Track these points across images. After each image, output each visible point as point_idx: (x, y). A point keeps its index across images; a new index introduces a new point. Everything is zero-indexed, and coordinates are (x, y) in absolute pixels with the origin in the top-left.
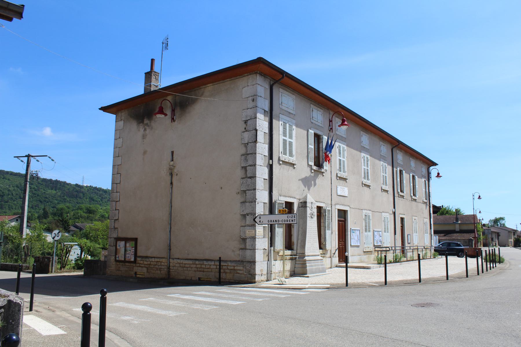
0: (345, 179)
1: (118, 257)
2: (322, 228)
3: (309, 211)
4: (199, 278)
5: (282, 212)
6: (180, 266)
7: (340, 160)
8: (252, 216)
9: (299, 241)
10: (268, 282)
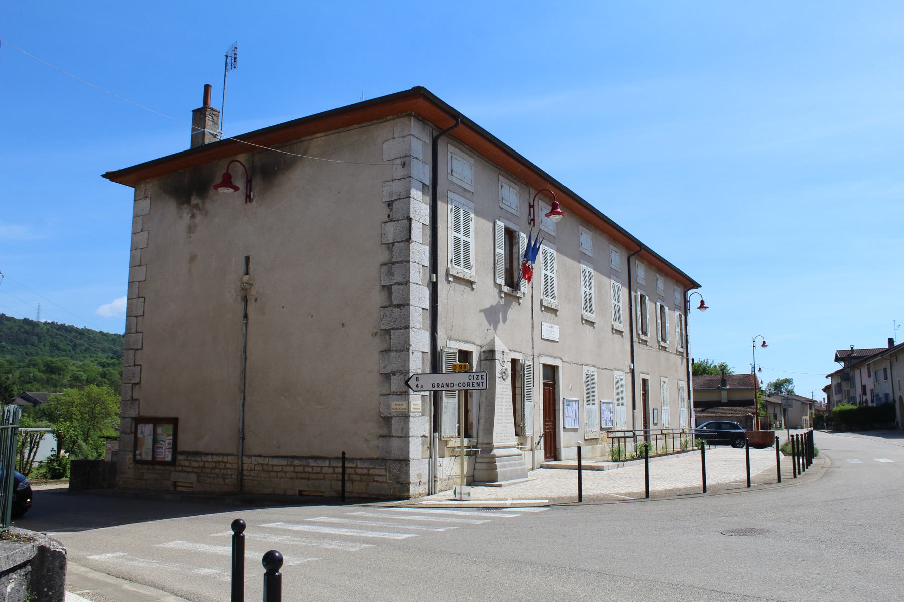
1: (140, 454)
2: (518, 398)
3: (498, 368)
4: (300, 491)
5: (458, 368)
6: (263, 470)
7: (546, 276)
8: (402, 376)
9: (482, 422)
10: (431, 497)
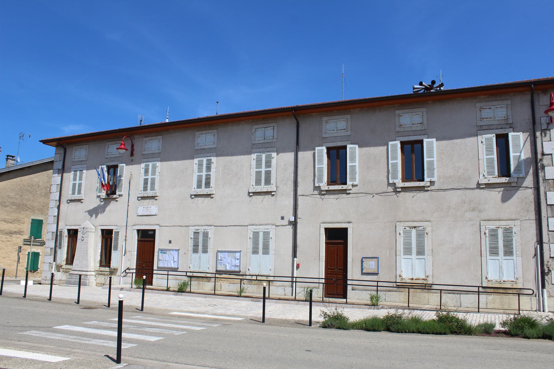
0: (153, 197)
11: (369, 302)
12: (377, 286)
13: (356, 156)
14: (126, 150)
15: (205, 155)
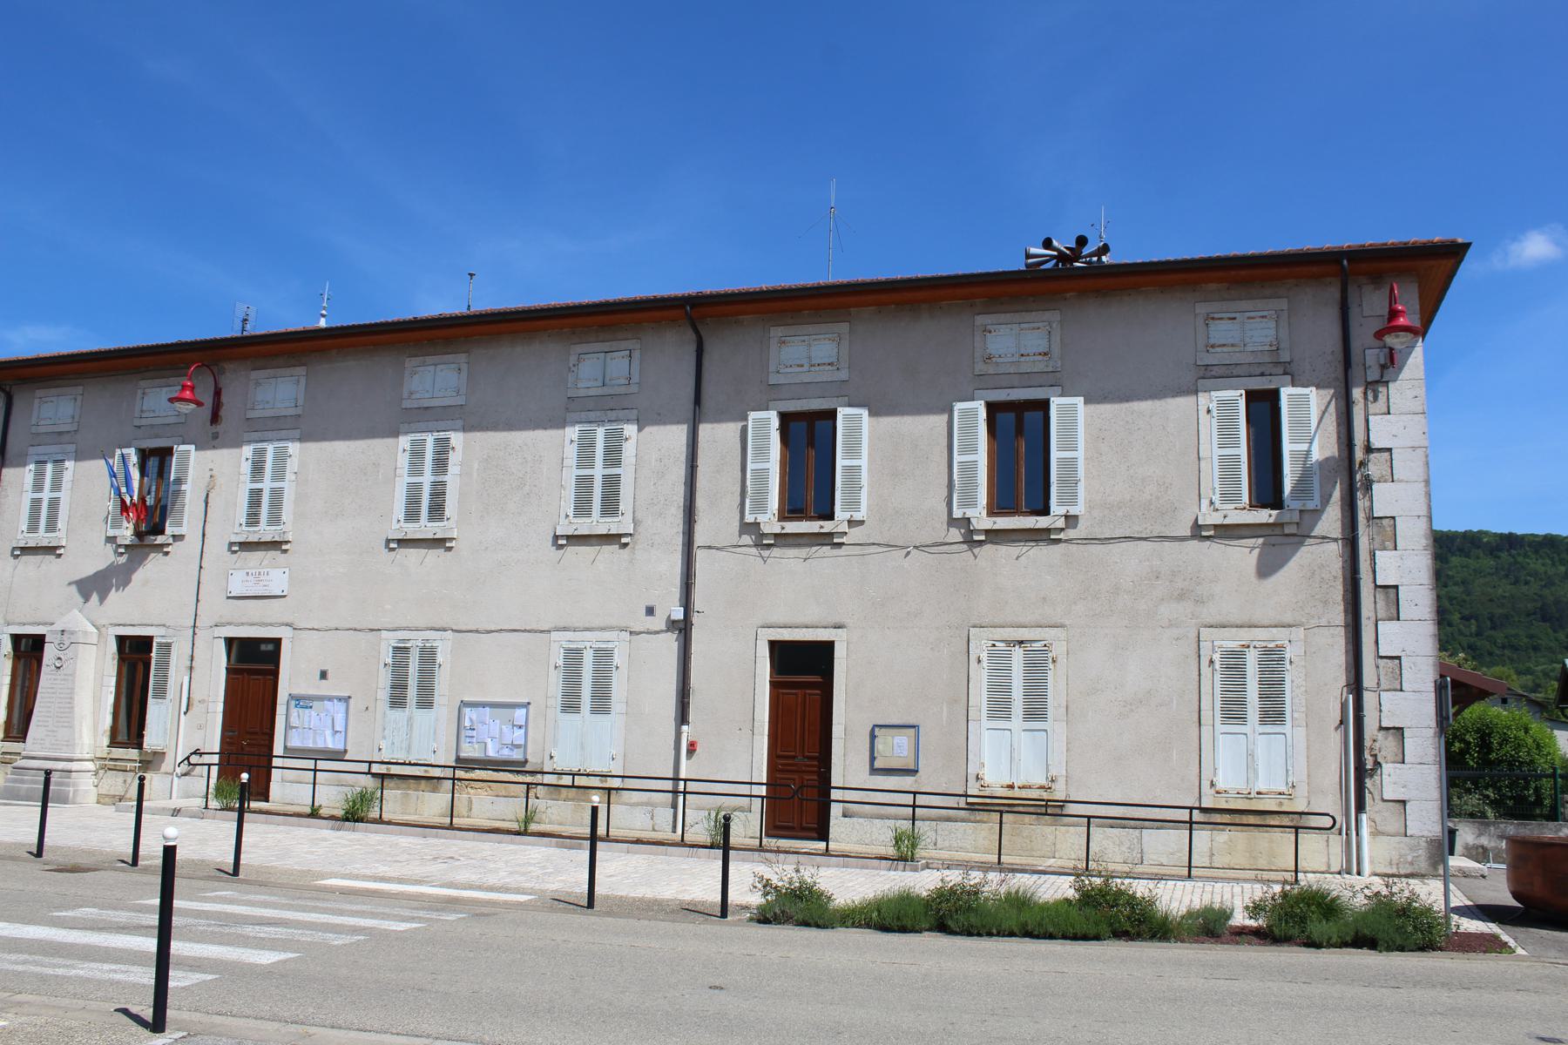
0: (275, 545)
11: (891, 851)
12: (914, 806)
13: (861, 438)
14: (199, 404)
15: (431, 425)
